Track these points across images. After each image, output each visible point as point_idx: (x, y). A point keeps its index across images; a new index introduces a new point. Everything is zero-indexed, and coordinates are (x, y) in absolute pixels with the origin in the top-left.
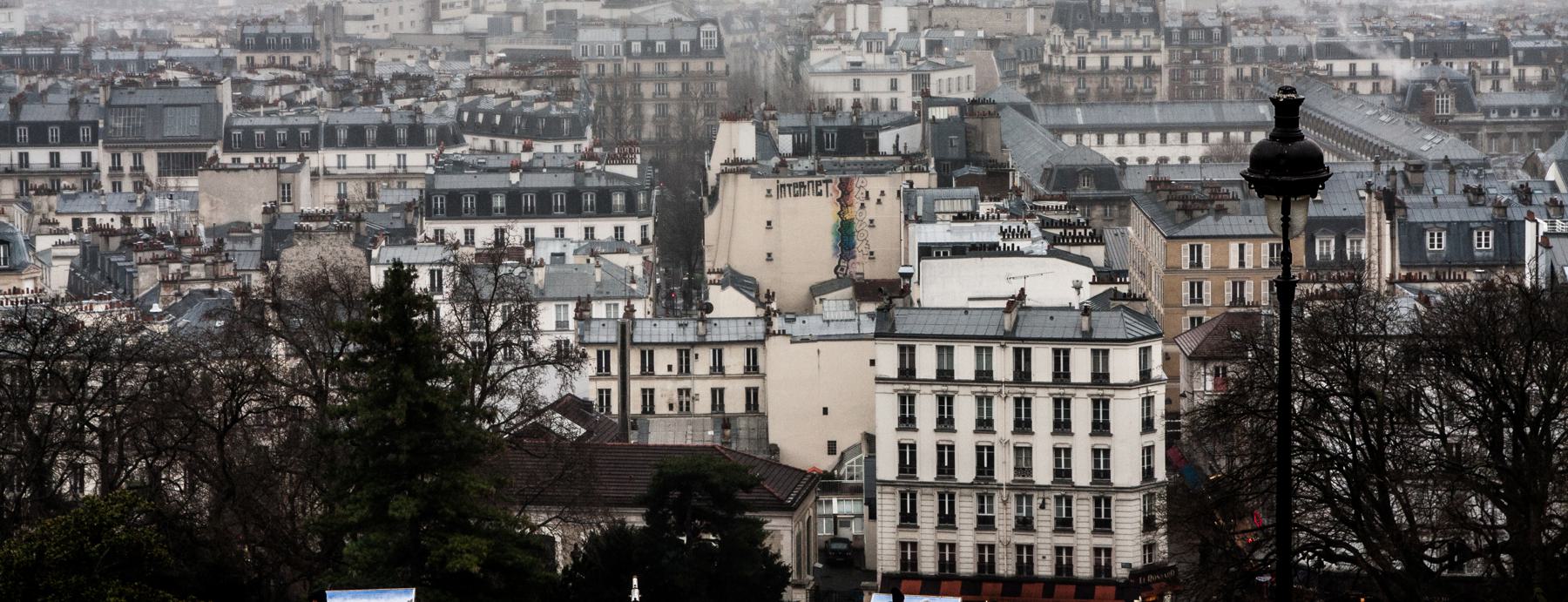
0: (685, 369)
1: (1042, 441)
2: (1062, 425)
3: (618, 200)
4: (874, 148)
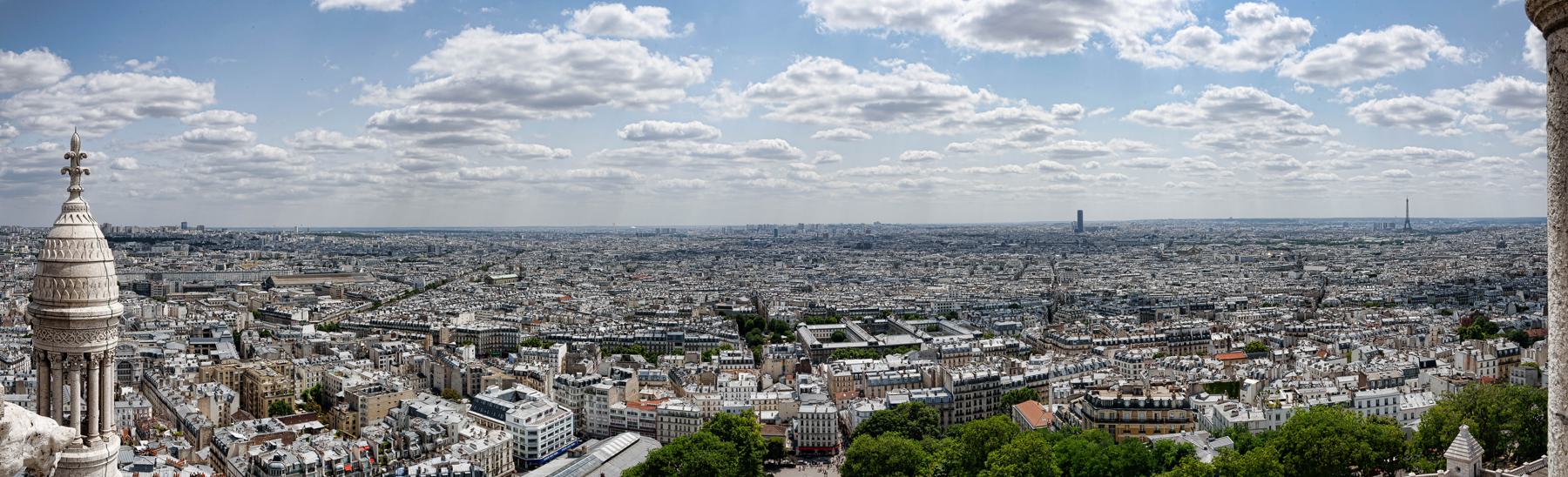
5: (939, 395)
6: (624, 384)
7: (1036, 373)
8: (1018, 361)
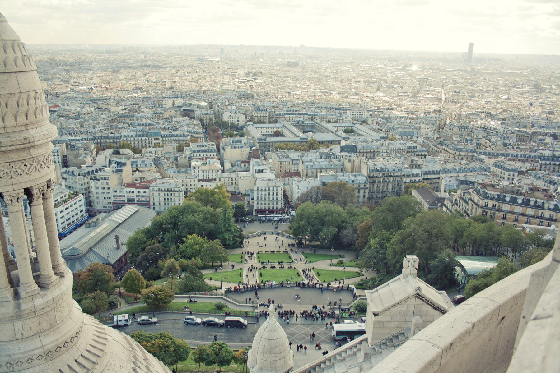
0: (229, 180)
1: (271, 196)
2: (273, 195)
3: (213, 151)
4: (241, 142)
5: (358, 178)
6: (121, 171)
7: (431, 169)
8: (416, 159)
